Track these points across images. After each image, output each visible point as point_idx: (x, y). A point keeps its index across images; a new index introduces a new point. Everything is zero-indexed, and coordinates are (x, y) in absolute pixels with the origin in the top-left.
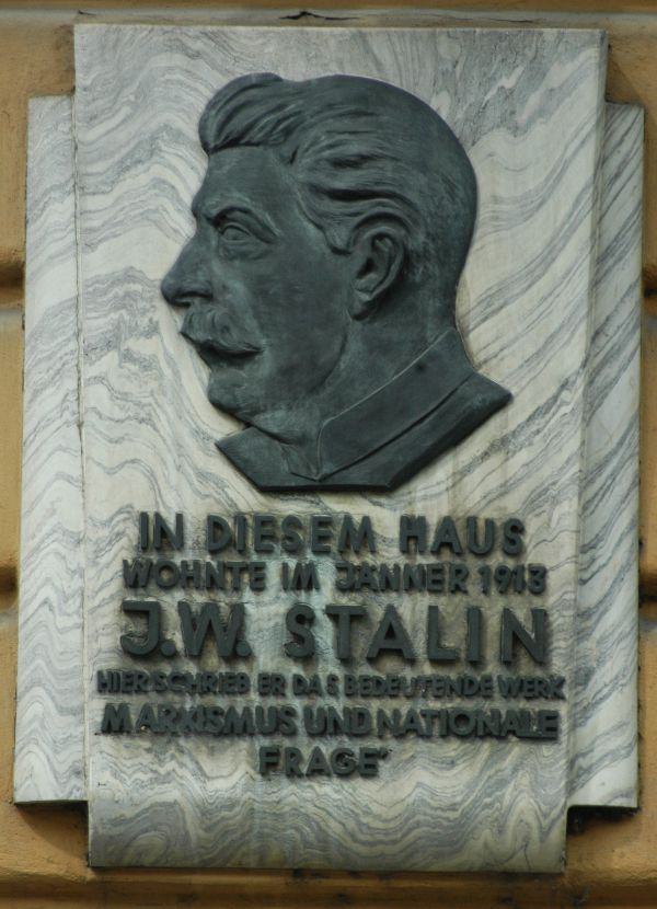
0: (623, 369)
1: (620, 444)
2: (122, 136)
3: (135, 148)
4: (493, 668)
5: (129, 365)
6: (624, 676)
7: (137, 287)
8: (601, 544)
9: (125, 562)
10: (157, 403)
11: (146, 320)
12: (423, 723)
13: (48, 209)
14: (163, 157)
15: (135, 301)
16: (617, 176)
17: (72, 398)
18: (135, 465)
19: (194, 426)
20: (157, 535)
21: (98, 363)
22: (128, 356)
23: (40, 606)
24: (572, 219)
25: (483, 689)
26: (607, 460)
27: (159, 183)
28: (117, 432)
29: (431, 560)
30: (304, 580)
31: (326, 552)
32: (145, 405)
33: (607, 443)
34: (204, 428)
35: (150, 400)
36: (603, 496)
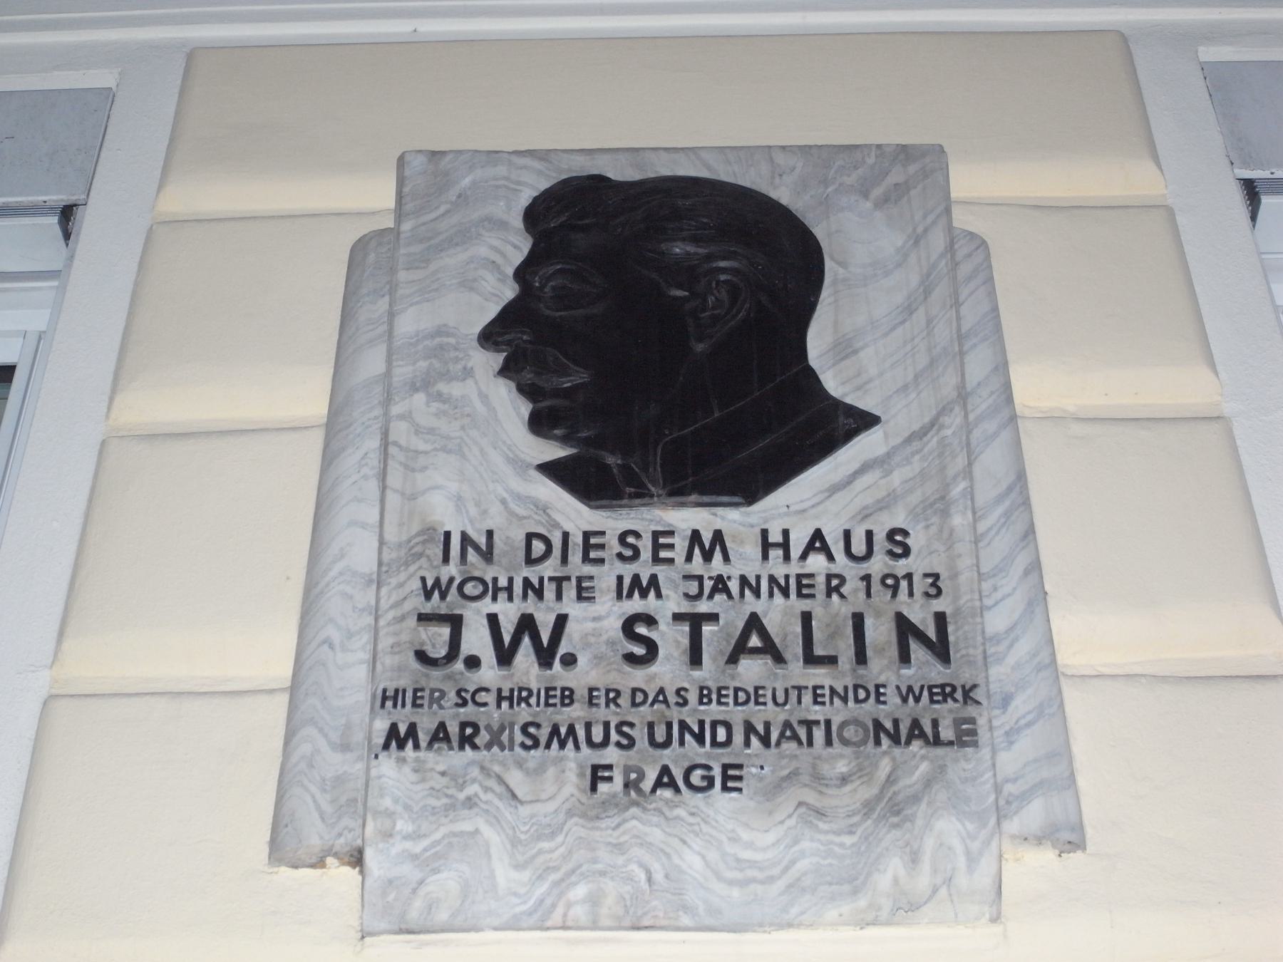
4: (882, 668)
9: (423, 579)
29: (794, 569)
34: (522, 456)
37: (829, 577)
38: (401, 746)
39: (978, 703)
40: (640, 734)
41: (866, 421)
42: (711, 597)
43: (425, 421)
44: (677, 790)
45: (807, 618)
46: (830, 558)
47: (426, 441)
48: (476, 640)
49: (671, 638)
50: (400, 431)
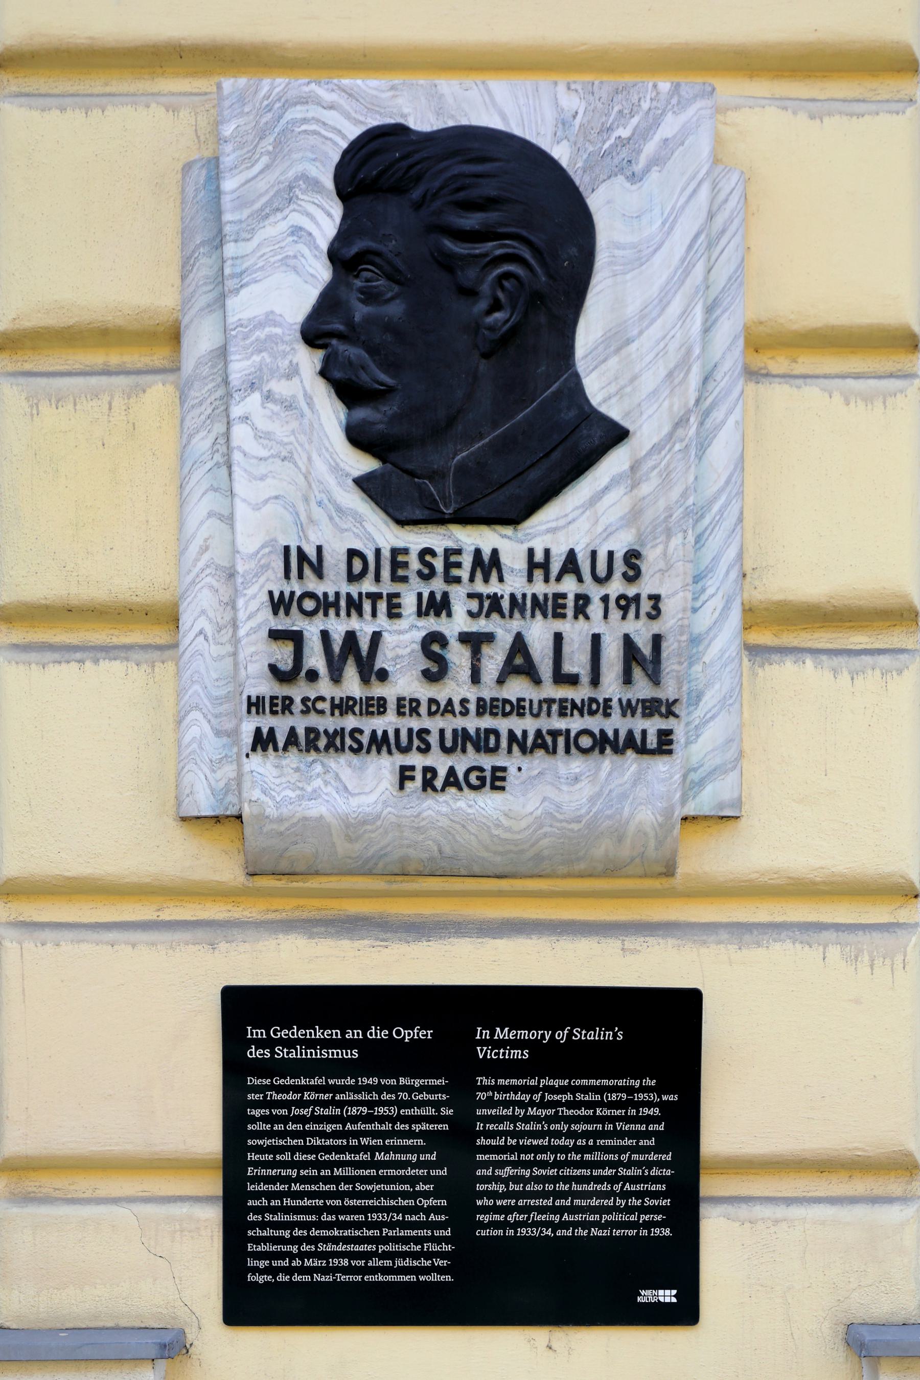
0: (730, 412)
1: (727, 482)
2: (262, 185)
3: (275, 195)
4: (611, 686)
5: (270, 405)
6: (731, 697)
7: (278, 331)
8: (710, 575)
9: (271, 593)
10: (297, 441)
11: (287, 362)
12: (549, 740)
13: (198, 264)
14: (300, 206)
15: (277, 344)
16: (723, 232)
17: (222, 441)
18: (277, 501)
19: (333, 464)
20: (304, 562)
21: (242, 404)
22: (268, 397)
23: (196, 636)
24: (686, 263)
25: (606, 708)
26: (715, 499)
27: (296, 231)
28: (263, 469)
29: (553, 588)
30: (438, 606)
31: (458, 580)
32: (286, 444)
33: (715, 481)
34: (342, 465)
35: (292, 439)
36: (713, 530)
37: (578, 597)
38: (265, 749)
39: (677, 716)
40: (433, 739)
41: (617, 435)
42: (488, 616)
43: (262, 424)
44: (460, 789)
45: (558, 638)
46: (580, 580)
47: (264, 447)
48: (315, 659)
49: (458, 657)
50: (240, 433)
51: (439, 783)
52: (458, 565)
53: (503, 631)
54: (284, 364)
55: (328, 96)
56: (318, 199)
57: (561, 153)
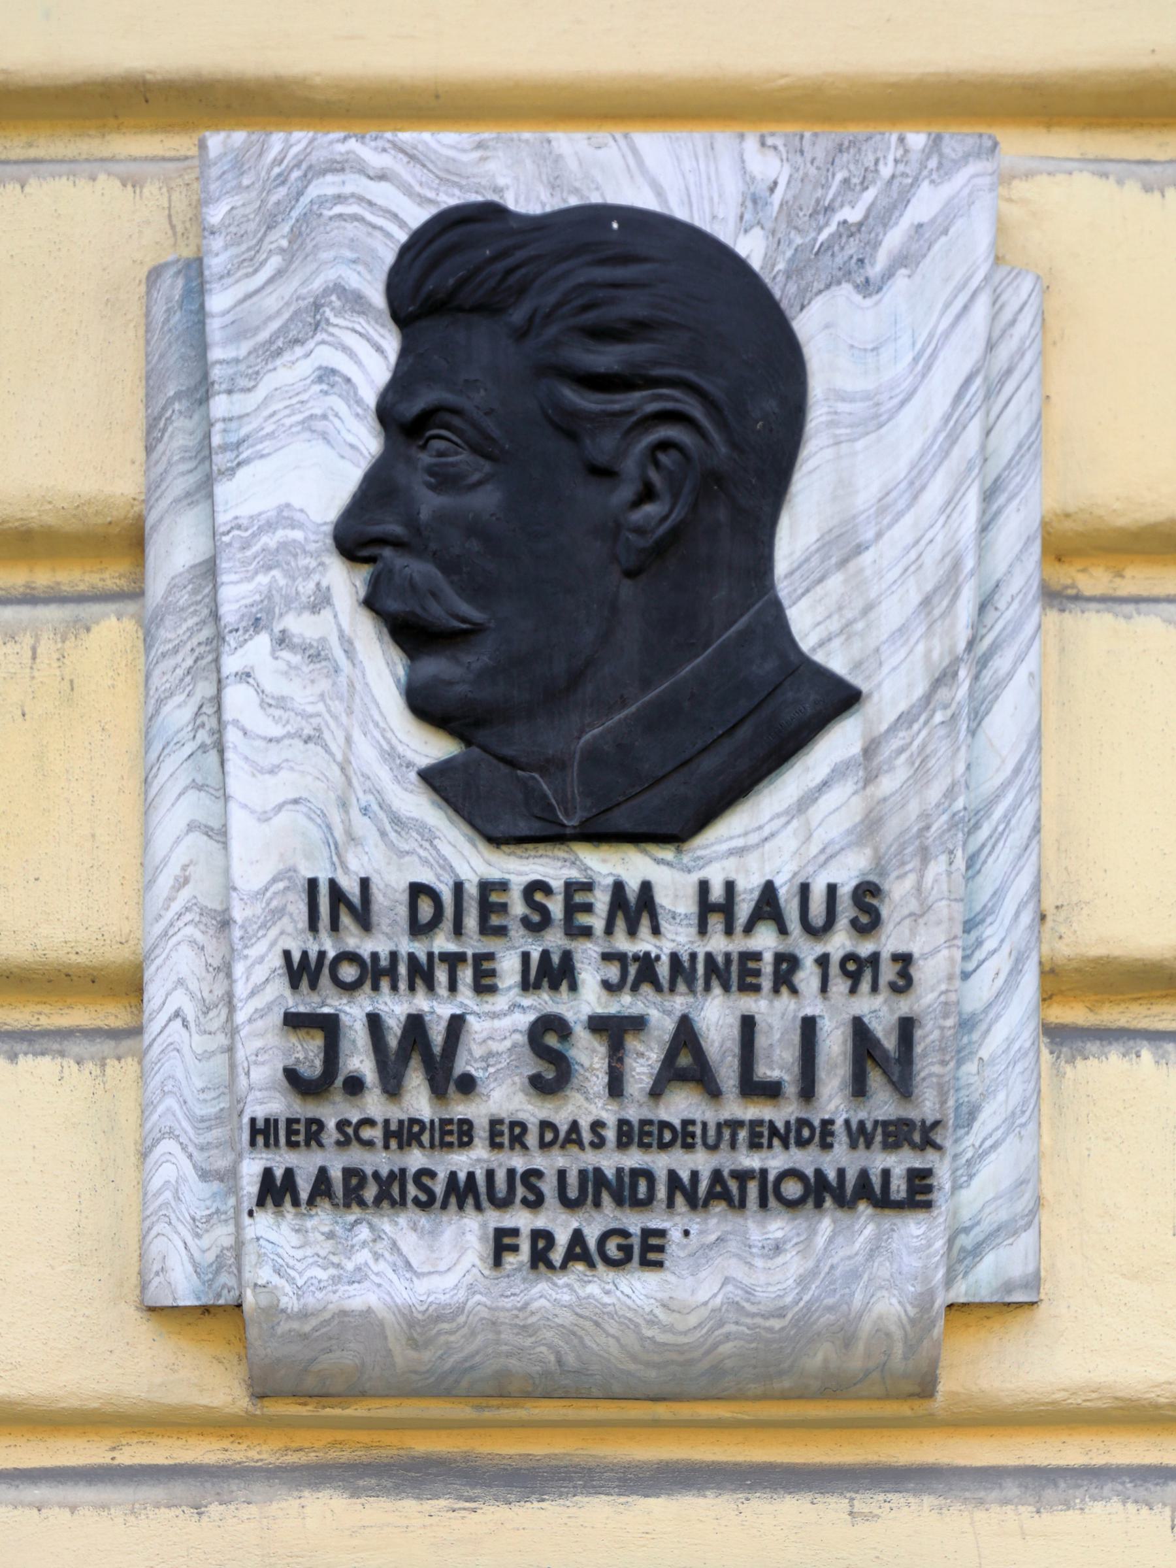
0: (1020, 659)
1: (1017, 771)
2: (271, 302)
3: (291, 319)
4: (833, 1101)
5: (285, 654)
6: (1023, 1112)
7: (298, 535)
8: (989, 920)
9: (287, 954)
10: (329, 711)
11: (311, 585)
12: (733, 1186)
13: (170, 429)
14: (332, 335)
15: (295, 556)
16: (1009, 372)
17: (209, 710)
18: (297, 807)
19: (386, 747)
20: (338, 904)
21: (240, 651)
22: (283, 640)
23: (170, 1020)
24: (952, 423)
25: (825, 1135)
26: (997, 797)
27: (326, 375)
28: (273, 756)
29: (739, 944)
30: (555, 974)
31: (587, 932)
32: (311, 716)
33: (998, 770)
34: (400, 749)
35: (320, 707)
36: (993, 848)
37: (779, 958)
38: (278, 1203)
40: (548, 1187)
41: (843, 698)
42: (635, 988)
43: (273, 684)
45: (748, 1024)
46: (783, 931)
47: (276, 720)
48: (359, 1060)
49: (588, 1054)
50: (237, 699)
51: (557, 1256)
52: (588, 908)
53: (660, 1012)
54: (307, 588)
55: (375, 159)
56: (361, 323)
57: (751, 248)
